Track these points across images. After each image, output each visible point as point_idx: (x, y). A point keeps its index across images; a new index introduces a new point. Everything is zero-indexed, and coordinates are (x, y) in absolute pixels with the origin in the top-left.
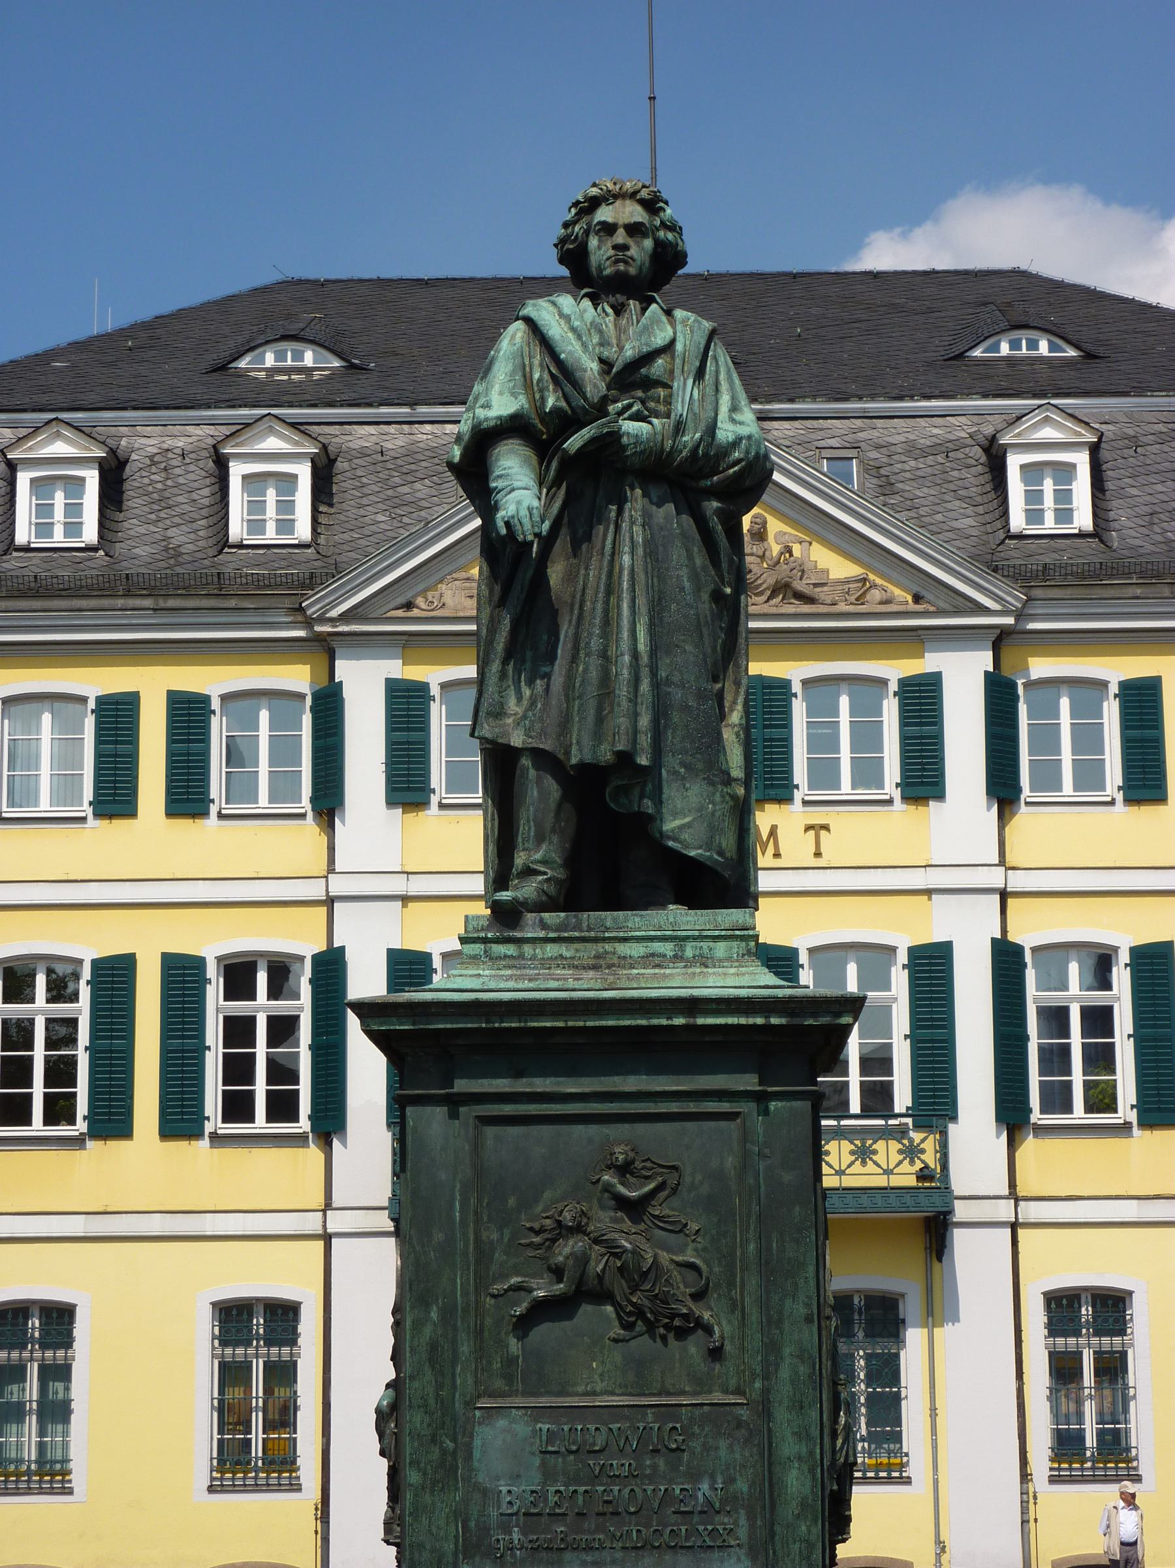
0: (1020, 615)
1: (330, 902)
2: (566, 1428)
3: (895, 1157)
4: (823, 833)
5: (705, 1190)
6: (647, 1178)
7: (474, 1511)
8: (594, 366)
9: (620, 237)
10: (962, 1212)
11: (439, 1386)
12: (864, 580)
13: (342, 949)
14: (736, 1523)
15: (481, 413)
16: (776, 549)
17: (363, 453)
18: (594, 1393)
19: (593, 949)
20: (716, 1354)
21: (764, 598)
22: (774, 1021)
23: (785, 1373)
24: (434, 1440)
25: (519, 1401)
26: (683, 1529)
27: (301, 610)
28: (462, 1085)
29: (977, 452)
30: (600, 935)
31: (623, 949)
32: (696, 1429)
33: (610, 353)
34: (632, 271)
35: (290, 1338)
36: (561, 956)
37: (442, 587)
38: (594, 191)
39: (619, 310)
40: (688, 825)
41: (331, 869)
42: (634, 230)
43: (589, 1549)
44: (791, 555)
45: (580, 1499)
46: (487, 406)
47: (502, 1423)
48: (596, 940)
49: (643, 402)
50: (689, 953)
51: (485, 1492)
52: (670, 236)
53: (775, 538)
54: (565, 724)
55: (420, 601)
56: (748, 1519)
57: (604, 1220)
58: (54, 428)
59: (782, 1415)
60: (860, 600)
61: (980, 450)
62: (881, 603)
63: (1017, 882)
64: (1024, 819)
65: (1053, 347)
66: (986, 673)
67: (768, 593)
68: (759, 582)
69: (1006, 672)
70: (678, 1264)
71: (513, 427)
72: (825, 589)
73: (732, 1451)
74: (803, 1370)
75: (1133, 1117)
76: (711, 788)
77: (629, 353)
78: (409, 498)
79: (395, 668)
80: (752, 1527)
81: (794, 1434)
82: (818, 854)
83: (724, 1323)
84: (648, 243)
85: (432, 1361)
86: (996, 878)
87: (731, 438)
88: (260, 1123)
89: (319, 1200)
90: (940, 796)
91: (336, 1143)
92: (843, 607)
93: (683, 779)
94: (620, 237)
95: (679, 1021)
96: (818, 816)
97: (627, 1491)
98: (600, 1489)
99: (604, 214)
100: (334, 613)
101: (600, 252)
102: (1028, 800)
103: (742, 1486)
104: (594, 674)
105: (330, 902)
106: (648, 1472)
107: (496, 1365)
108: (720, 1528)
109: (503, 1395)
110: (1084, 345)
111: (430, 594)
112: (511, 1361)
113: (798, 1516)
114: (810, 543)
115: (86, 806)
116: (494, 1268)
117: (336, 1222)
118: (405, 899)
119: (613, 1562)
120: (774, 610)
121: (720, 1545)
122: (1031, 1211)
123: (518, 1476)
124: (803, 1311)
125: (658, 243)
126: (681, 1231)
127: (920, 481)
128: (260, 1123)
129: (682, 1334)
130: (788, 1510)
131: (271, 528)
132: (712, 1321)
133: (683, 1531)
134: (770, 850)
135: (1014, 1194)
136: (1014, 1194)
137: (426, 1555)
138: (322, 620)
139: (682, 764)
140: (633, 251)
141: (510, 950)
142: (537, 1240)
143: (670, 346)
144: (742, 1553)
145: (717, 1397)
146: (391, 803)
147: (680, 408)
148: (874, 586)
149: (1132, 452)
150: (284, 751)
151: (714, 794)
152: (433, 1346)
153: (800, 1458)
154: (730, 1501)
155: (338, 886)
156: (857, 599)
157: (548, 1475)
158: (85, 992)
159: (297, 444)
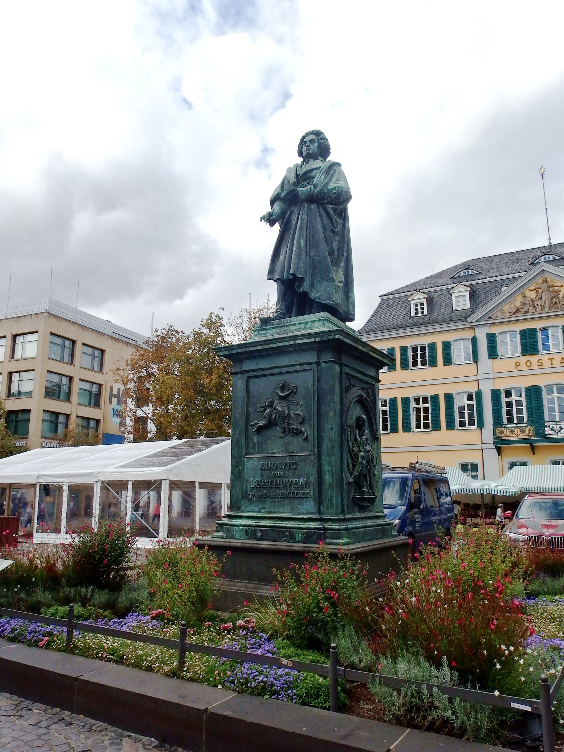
1: (478, 380)
2: (266, 463)
5: (303, 392)
6: (288, 390)
7: (245, 486)
11: (238, 452)
14: (310, 491)
18: (275, 453)
19: (284, 329)
20: (306, 439)
22: (317, 339)
23: (325, 445)
24: (237, 467)
25: (256, 456)
26: (296, 492)
28: (245, 368)
30: (285, 324)
31: (291, 328)
32: (300, 463)
34: (311, 152)
36: (277, 332)
40: (322, 295)
42: (312, 141)
43: (272, 498)
45: (270, 483)
47: (251, 462)
48: (284, 326)
50: (308, 326)
51: (247, 481)
52: (322, 141)
56: (313, 489)
58: (417, 292)
59: (324, 458)
70: (296, 414)
73: (309, 469)
74: (330, 444)
76: (328, 283)
79: (488, 330)
80: (314, 492)
81: (327, 464)
83: (308, 431)
85: (237, 445)
87: (332, 187)
88: (467, 427)
89: (480, 442)
93: (320, 282)
95: (292, 343)
97: (281, 481)
98: (275, 480)
100: (474, 321)
103: (312, 479)
105: (478, 380)
106: (287, 475)
107: (251, 446)
108: (305, 492)
109: (252, 454)
112: (255, 444)
113: (328, 489)
115: (427, 366)
116: (251, 418)
117: (484, 446)
119: (278, 501)
121: (305, 497)
123: (255, 477)
124: (330, 427)
125: (318, 142)
126: (297, 405)
128: (467, 427)
129: (297, 434)
130: (326, 487)
132: (304, 431)
133: (296, 492)
137: (235, 498)
139: (320, 278)
140: (312, 147)
141: (264, 332)
142: (261, 410)
144: (311, 499)
145: (306, 453)
151: (329, 285)
152: (237, 441)
153: (329, 471)
154: (307, 484)
155: (479, 377)
157: (262, 476)
158: (429, 402)
159: (466, 289)
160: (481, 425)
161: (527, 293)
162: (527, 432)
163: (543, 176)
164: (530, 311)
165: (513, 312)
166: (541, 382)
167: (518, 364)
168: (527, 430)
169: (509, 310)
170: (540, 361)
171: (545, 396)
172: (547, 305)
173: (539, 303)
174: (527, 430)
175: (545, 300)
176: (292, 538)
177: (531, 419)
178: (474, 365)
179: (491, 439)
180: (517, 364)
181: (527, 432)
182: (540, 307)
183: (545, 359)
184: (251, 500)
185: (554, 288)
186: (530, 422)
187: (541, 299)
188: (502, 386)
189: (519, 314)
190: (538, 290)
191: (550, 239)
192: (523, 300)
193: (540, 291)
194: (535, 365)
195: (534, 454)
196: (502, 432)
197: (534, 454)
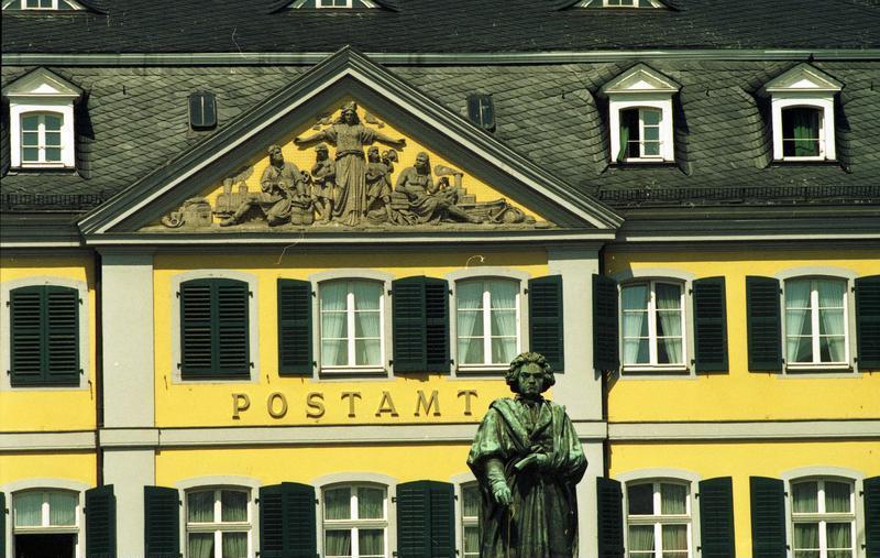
0: (618, 232)
1: (99, 451)
4: (472, 396)
8: (526, 433)
9: (531, 379)
12: (502, 204)
13: (111, 487)
15: (483, 449)
16: (435, 179)
17: (110, 91)
21: (427, 218)
27: (78, 229)
29: (586, 95)
33: (530, 426)
37: (183, 209)
38: (521, 359)
39: (532, 406)
42: (536, 376)
44: (448, 184)
46: (485, 446)
49: (542, 445)
53: (435, 170)
55: (165, 219)
60: (500, 219)
61: (588, 92)
62: (515, 222)
63: (616, 432)
64: (622, 386)
66: (594, 275)
67: (431, 214)
68: (424, 206)
71: (495, 455)
72: (474, 210)
77: (538, 427)
78: (148, 130)
84: (541, 380)
94: (531, 379)
99: (525, 369)
100: (101, 231)
101: (525, 384)
102: (626, 369)
104: (528, 550)
111: (173, 214)
114: (462, 175)
118: (158, 449)
120: (435, 228)
127: (542, 118)
131: (42, 154)
134: (432, 410)
140: (537, 384)
143: (551, 422)
147: (557, 449)
148: (510, 208)
149: (703, 95)
156: (497, 219)
161: (289, 152)
164: (295, 219)
165: (238, 212)
166: (314, 470)
167: (242, 403)
169: (225, 202)
170: (315, 399)
171: (323, 520)
172: (351, 205)
173: (331, 193)
175: (345, 190)
182: (328, 206)
185: (376, 144)
187: (332, 178)
188: (181, 473)
189: (255, 226)
190: (325, 143)
192: (275, 174)
193: (332, 151)
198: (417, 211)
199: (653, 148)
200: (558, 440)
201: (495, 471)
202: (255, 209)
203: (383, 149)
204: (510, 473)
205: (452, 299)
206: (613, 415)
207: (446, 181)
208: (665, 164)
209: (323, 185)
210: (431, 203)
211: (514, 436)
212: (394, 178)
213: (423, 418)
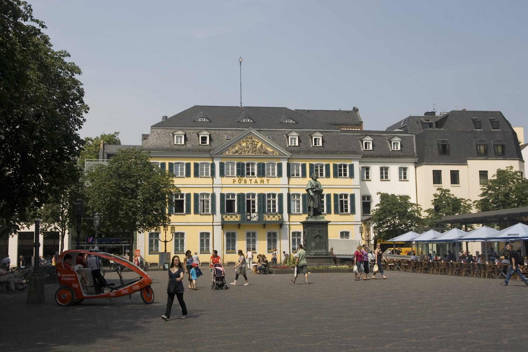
3: (277, 217)
10: (284, 223)
35: (209, 236)
41: (213, 184)
54: (314, 206)
57: (317, 233)
60: (273, 154)
63: (290, 186)
65: (292, 121)
69: (289, 162)
75: (302, 213)
82: (268, 183)
86: (288, 186)
90: (282, 177)
91: (214, 215)
92: (271, 155)
96: (268, 179)
99: (314, 176)
101: (314, 178)
110: (296, 121)
117: (214, 224)
118: (222, 187)
122: (291, 223)
135: (289, 221)
136: (289, 221)
138: (212, 155)
146: (220, 176)
150: (207, 170)
155: (214, 186)
160: (214, 212)
162: (239, 218)
163: (241, 63)
168: (239, 216)
174: (239, 216)
176: (323, 255)
177: (239, 210)
178: (211, 179)
179: (220, 221)
180: (234, 181)
181: (239, 218)
183: (248, 179)
184: (313, 249)
186: (239, 212)
187: (248, 147)
191: (241, 103)
193: (248, 143)
194: (243, 182)
195: (239, 228)
196: (226, 217)
197: (239, 228)
198: (261, 152)
199: (319, 144)
200: (319, 186)
201: (310, 191)
202: (237, 151)
203: (256, 143)
204: (313, 192)
205: (266, 166)
206: (290, 184)
207: (265, 148)
208: (321, 147)
209: (247, 148)
210: (263, 151)
211: (313, 186)
212: (257, 147)
213: (261, 184)
